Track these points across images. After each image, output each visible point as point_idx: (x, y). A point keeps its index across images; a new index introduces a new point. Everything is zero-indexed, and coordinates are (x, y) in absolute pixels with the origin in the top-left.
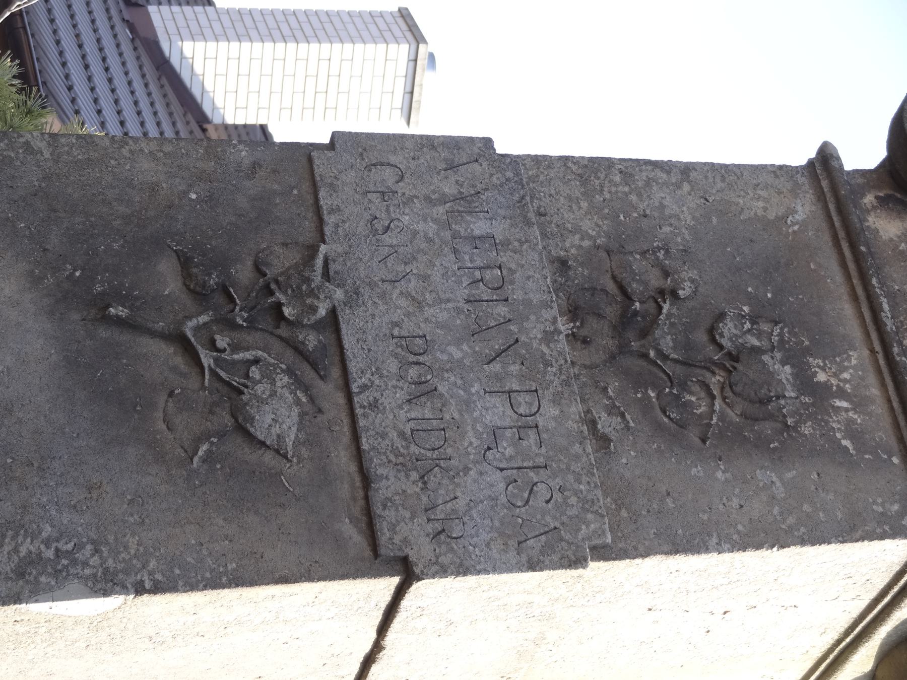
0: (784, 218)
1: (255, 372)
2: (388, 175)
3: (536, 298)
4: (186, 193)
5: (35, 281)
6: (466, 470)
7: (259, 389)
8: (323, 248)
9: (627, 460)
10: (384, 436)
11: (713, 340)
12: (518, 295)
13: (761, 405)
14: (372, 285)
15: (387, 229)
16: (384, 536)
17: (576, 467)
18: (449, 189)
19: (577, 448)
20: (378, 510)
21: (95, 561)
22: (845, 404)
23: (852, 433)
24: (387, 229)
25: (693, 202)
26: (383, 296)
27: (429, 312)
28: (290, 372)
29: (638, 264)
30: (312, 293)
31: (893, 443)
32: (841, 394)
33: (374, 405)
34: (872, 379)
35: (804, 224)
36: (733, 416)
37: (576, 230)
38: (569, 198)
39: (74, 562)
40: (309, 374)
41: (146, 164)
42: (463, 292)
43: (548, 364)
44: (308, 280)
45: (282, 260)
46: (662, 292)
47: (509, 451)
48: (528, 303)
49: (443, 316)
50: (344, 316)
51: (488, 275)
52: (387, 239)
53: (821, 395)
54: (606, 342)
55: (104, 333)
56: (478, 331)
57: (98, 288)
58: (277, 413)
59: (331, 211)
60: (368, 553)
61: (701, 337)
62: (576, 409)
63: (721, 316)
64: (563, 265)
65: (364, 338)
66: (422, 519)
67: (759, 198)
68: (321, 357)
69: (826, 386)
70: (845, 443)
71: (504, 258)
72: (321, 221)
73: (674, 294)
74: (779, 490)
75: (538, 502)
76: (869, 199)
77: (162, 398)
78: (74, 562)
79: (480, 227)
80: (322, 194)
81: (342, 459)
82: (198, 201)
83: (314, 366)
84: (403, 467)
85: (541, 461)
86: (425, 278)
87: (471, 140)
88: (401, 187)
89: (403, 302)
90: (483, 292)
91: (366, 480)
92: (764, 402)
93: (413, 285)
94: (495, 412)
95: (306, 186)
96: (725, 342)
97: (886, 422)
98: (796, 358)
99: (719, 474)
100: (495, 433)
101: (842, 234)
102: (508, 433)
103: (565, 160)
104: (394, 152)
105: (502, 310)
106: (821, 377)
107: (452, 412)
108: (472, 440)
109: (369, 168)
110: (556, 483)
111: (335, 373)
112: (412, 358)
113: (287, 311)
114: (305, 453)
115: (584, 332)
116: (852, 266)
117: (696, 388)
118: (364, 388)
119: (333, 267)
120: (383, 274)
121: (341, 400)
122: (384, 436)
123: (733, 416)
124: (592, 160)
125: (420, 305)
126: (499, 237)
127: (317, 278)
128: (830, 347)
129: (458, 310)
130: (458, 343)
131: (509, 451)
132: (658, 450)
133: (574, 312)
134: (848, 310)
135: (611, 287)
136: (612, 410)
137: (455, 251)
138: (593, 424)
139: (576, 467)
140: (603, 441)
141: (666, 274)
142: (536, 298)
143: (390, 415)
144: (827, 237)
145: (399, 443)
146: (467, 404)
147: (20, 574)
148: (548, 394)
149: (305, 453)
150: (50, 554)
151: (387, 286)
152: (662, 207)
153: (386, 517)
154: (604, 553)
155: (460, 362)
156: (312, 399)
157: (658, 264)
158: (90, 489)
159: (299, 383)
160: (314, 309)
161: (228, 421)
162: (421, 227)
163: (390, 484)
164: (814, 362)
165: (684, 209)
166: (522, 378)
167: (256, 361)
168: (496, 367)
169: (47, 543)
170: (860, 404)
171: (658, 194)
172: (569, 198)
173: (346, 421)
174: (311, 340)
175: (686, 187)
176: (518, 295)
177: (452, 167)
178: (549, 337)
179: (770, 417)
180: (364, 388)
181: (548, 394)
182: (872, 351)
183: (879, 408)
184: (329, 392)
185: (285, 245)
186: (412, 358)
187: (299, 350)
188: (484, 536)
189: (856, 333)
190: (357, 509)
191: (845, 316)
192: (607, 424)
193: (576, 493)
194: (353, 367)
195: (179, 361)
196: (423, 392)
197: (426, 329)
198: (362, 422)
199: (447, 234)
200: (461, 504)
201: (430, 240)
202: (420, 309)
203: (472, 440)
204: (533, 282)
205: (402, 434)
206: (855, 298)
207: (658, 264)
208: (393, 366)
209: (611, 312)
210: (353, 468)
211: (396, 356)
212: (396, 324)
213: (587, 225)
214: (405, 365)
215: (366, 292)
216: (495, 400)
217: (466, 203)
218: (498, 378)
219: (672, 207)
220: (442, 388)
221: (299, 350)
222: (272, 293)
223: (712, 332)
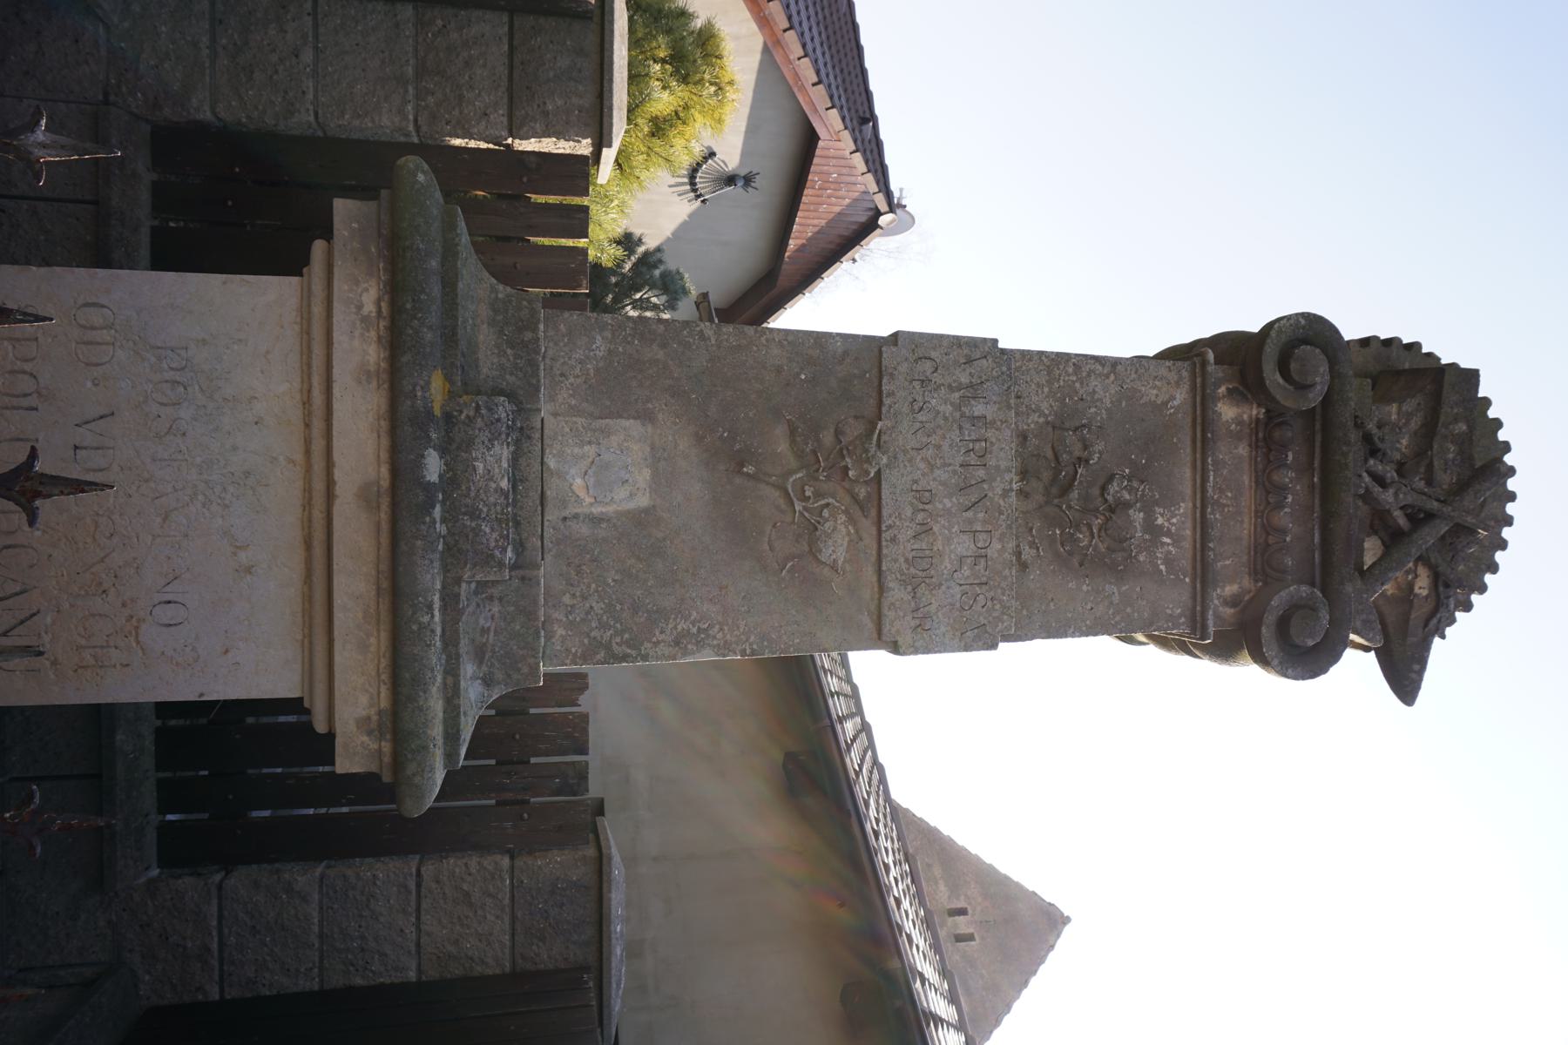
0: (1165, 404)
1: (826, 513)
2: (927, 366)
3: (1003, 464)
4: (798, 374)
5: (699, 439)
6: (941, 585)
7: (827, 525)
8: (880, 424)
9: (1034, 574)
10: (896, 561)
11: (1102, 495)
12: (993, 463)
14: (905, 452)
15: (921, 409)
16: (885, 630)
17: (1003, 584)
18: (964, 379)
19: (1007, 572)
20: (885, 611)
21: (720, 635)
22: (1168, 540)
23: (1168, 561)
24: (921, 409)
25: (1114, 389)
26: (910, 461)
27: (937, 472)
28: (846, 512)
29: (1070, 437)
30: (868, 461)
31: (1189, 568)
32: (1169, 534)
33: (894, 540)
34: (1189, 524)
35: (1177, 408)
36: (1102, 548)
37: (1038, 410)
38: (1038, 385)
39: (708, 636)
40: (857, 513)
41: (776, 351)
42: (960, 459)
43: (1001, 513)
44: (867, 451)
46: (1079, 459)
47: (967, 573)
48: (997, 467)
49: (944, 476)
50: (885, 474)
51: (977, 446)
52: (921, 417)
54: (1040, 498)
55: (738, 480)
56: (964, 489)
57: (737, 447)
58: (837, 545)
59: (889, 395)
60: (875, 635)
61: (1096, 491)
62: (1011, 545)
63: (1111, 478)
64: (1023, 437)
65: (896, 487)
66: (909, 618)
67: (1155, 387)
69: (1161, 527)
70: (1162, 567)
71: (990, 434)
72: (880, 404)
73: (1087, 461)
74: (1116, 599)
75: (977, 607)
76: (1222, 390)
77: (768, 528)
78: (708, 636)
79: (979, 409)
80: (885, 381)
81: (869, 574)
82: (805, 381)
83: (862, 509)
84: (903, 583)
85: (984, 579)
86: (938, 447)
87: (985, 340)
88: (937, 378)
89: (922, 465)
90: (973, 459)
91: (882, 589)
92: (1121, 542)
93: (930, 452)
95: (875, 371)
96: (1110, 498)
97: (1189, 555)
99: (1085, 588)
100: (961, 559)
101: (1199, 420)
102: (969, 561)
103: (1041, 353)
104: (934, 349)
105: (981, 473)
106: (1160, 521)
107: (939, 545)
108: (947, 565)
109: (916, 361)
110: (989, 595)
111: (873, 512)
112: (921, 506)
113: (851, 473)
114: (848, 568)
115: (1027, 489)
116: (1199, 444)
117: (1084, 529)
118: (889, 527)
119: (884, 438)
120: (913, 444)
121: (874, 531)
122: (896, 561)
123: (1102, 548)
124: (1058, 354)
125: (932, 467)
126: (989, 418)
127: (873, 449)
129: (955, 472)
130: (950, 496)
131: (967, 573)
132: (1054, 571)
133: (1024, 474)
134: (1188, 473)
135: (1049, 454)
136: (1032, 545)
137: (961, 428)
138: (1019, 554)
139: (1003, 584)
140: (1023, 566)
141: (1085, 448)
142: (1003, 464)
144: (1189, 420)
145: (904, 566)
146: (948, 540)
147: (677, 643)
148: (997, 534)
149: (848, 568)
150: (694, 630)
151: (914, 453)
152: (1094, 392)
153: (889, 614)
154: (1008, 638)
155: (949, 510)
156: (857, 532)
157: (1083, 440)
158: (721, 589)
159: (851, 520)
160: (868, 473)
161: (806, 548)
162: (941, 408)
164: (1159, 510)
166: (985, 522)
167: (828, 505)
168: (970, 514)
169: (693, 623)
170: (1177, 542)
171: (1094, 382)
172: (1038, 385)
173: (875, 546)
174: (862, 492)
175: (1112, 377)
176: (993, 463)
177: (969, 361)
178: (1005, 493)
179: (1124, 550)
180: (889, 527)
181: (997, 534)
182: (1195, 506)
183: (1187, 544)
185: (856, 417)
186: (921, 506)
187: (854, 498)
188: (943, 629)
189: (1189, 491)
190: (873, 607)
192: (1028, 553)
193: (1001, 601)
194: (885, 513)
195: (782, 502)
197: (933, 485)
198: (885, 551)
199: (958, 415)
200: (933, 608)
201: (946, 419)
202: (932, 471)
203: (947, 565)
204: (1004, 454)
205: (907, 560)
206: (1194, 467)
207: (1083, 440)
208: (909, 512)
209: (1046, 475)
210: (875, 579)
211: (912, 504)
212: (916, 482)
213: (1044, 406)
214: (916, 511)
215: (901, 456)
216: (965, 537)
217: (973, 391)
218: (970, 522)
219: (1100, 393)
220: (935, 529)
221: (854, 498)
222: (843, 457)
223: (1104, 489)
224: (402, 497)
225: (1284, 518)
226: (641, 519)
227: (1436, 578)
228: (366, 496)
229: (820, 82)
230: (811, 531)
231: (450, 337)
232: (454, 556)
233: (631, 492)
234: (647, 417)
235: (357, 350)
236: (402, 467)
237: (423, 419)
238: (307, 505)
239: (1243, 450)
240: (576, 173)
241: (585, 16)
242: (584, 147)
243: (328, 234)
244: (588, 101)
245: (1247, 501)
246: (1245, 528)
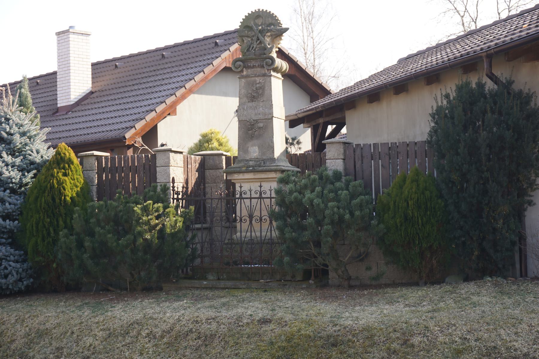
9: (265, 99)
13: (260, 88)
45: (248, 123)
53: (259, 83)
58: (261, 125)
65: (255, 118)
68: (257, 121)
94: (261, 109)
98: (257, 84)
128: (256, 81)
143: (261, 117)
163: (266, 117)
165: (243, 91)
184: (259, 121)
191: (253, 79)
196: (259, 114)
204: (250, 104)
217: (243, 109)
224: (254, 171)
225: (257, 65)
226: (259, 147)
227: (267, 32)
228: (254, 175)
229: (203, 71)
230: (260, 128)
231: (239, 167)
232: (260, 166)
233: (256, 149)
234: (248, 147)
235: (241, 176)
236: (251, 172)
237: (246, 170)
238: (256, 182)
239: (249, 70)
240: (228, 159)
241: (204, 158)
242: (224, 157)
243: (231, 180)
244: (216, 157)
245: (256, 69)
246: (259, 69)
